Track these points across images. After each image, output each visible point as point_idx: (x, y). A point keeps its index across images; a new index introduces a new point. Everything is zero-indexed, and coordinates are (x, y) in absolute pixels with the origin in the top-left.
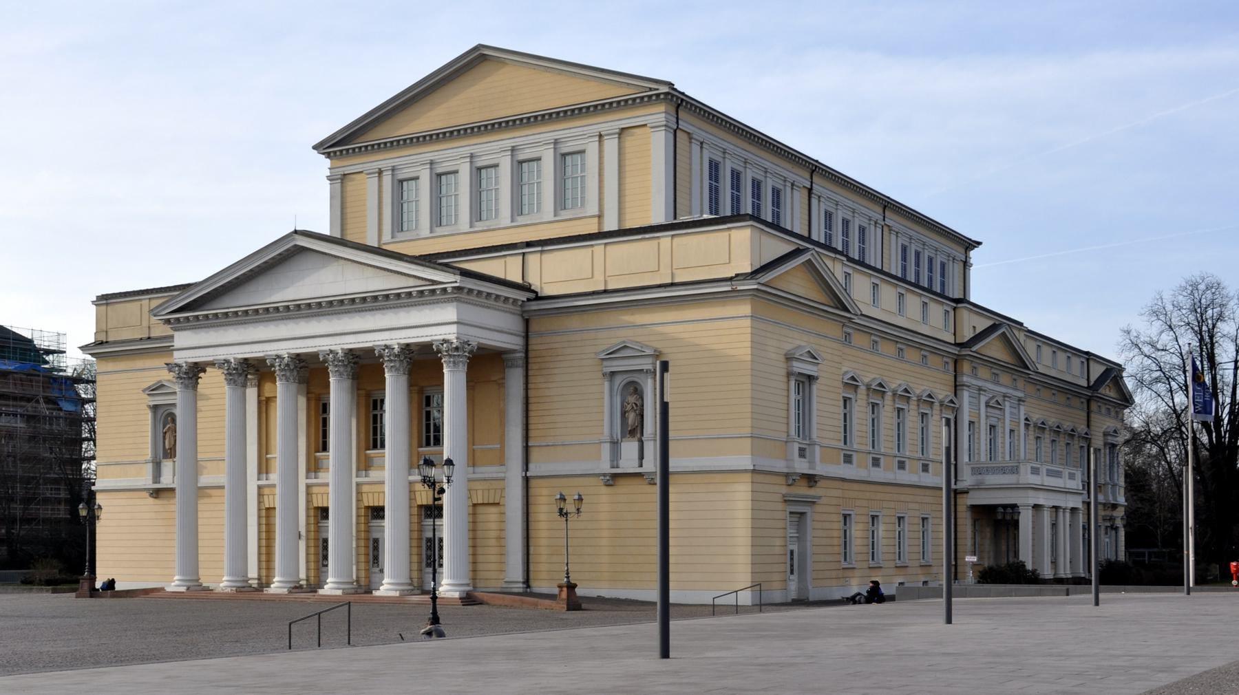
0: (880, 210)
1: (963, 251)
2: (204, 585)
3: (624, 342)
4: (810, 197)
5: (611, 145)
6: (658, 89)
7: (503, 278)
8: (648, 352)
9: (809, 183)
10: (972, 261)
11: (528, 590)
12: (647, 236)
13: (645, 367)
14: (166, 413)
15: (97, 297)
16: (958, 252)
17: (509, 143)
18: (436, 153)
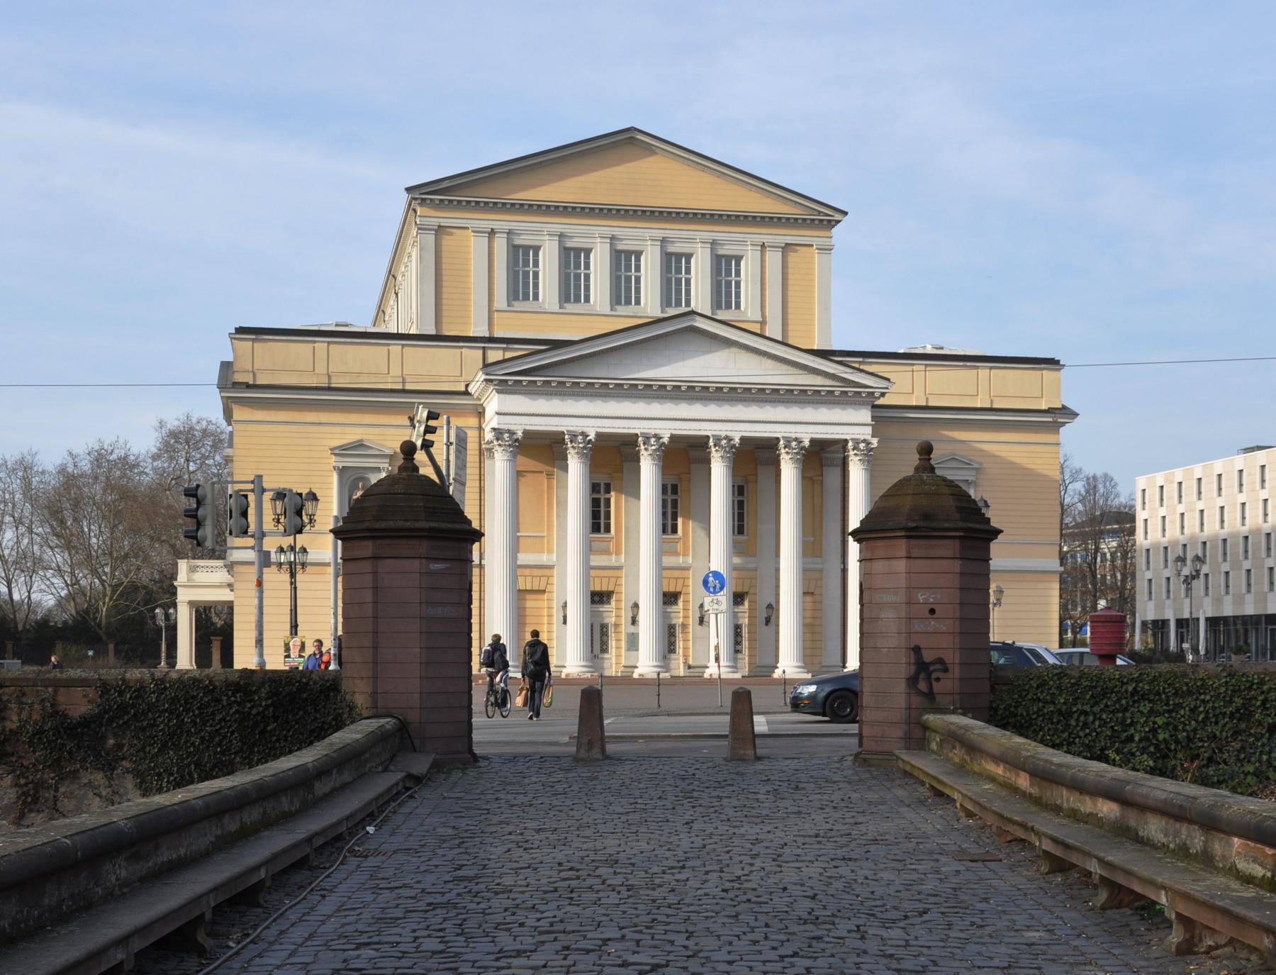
3: (954, 455)
5: (773, 259)
8: (975, 466)
12: (969, 364)
13: (970, 479)
14: (351, 479)
15: (236, 328)
18: (568, 227)
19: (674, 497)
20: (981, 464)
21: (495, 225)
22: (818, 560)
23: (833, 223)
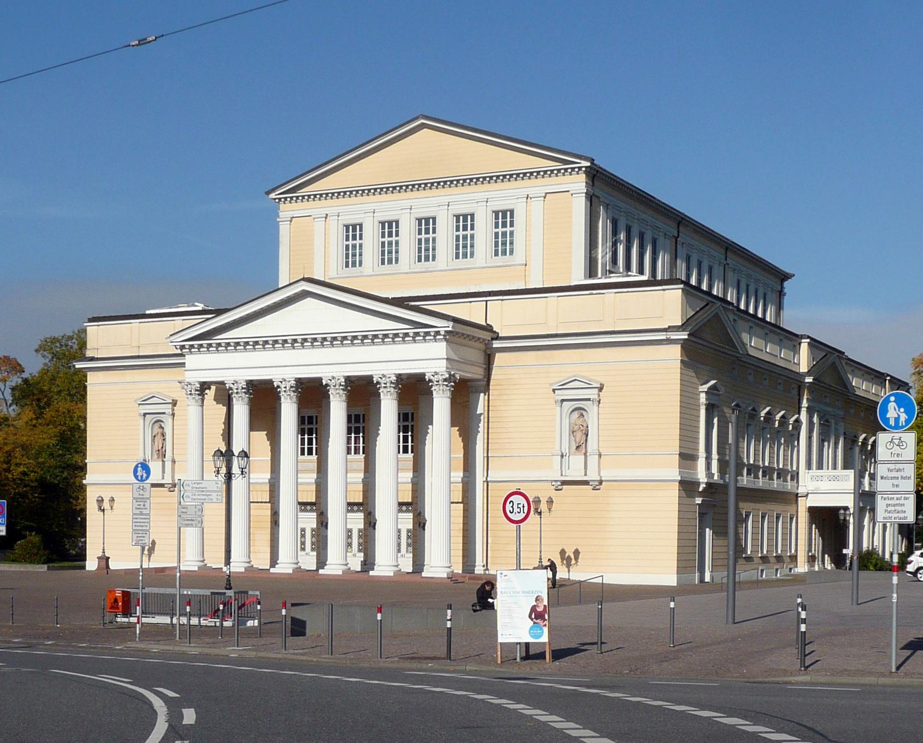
0: (723, 251)
1: (779, 282)
2: (208, 565)
4: (676, 243)
6: (580, 163)
7: (323, 280)
9: (676, 232)
10: (785, 290)
11: (487, 572)
16: (774, 283)
17: (446, 200)
18: (379, 204)
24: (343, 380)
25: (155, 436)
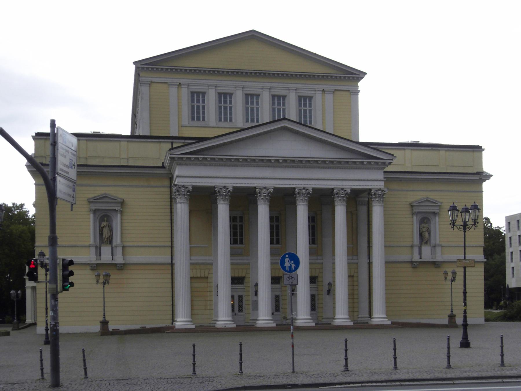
3: (427, 198)
8: (439, 204)
13: (436, 211)
14: (100, 216)
19: (277, 224)
20: (442, 203)
21: (181, 81)
22: (355, 257)
23: (360, 79)
24: (311, 191)
25: (103, 227)
